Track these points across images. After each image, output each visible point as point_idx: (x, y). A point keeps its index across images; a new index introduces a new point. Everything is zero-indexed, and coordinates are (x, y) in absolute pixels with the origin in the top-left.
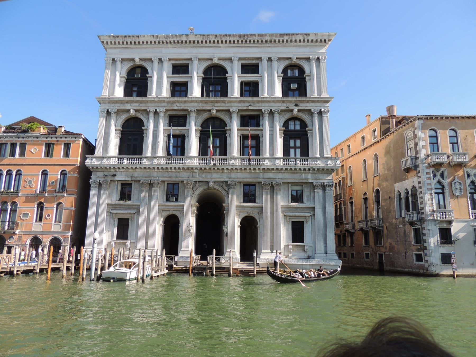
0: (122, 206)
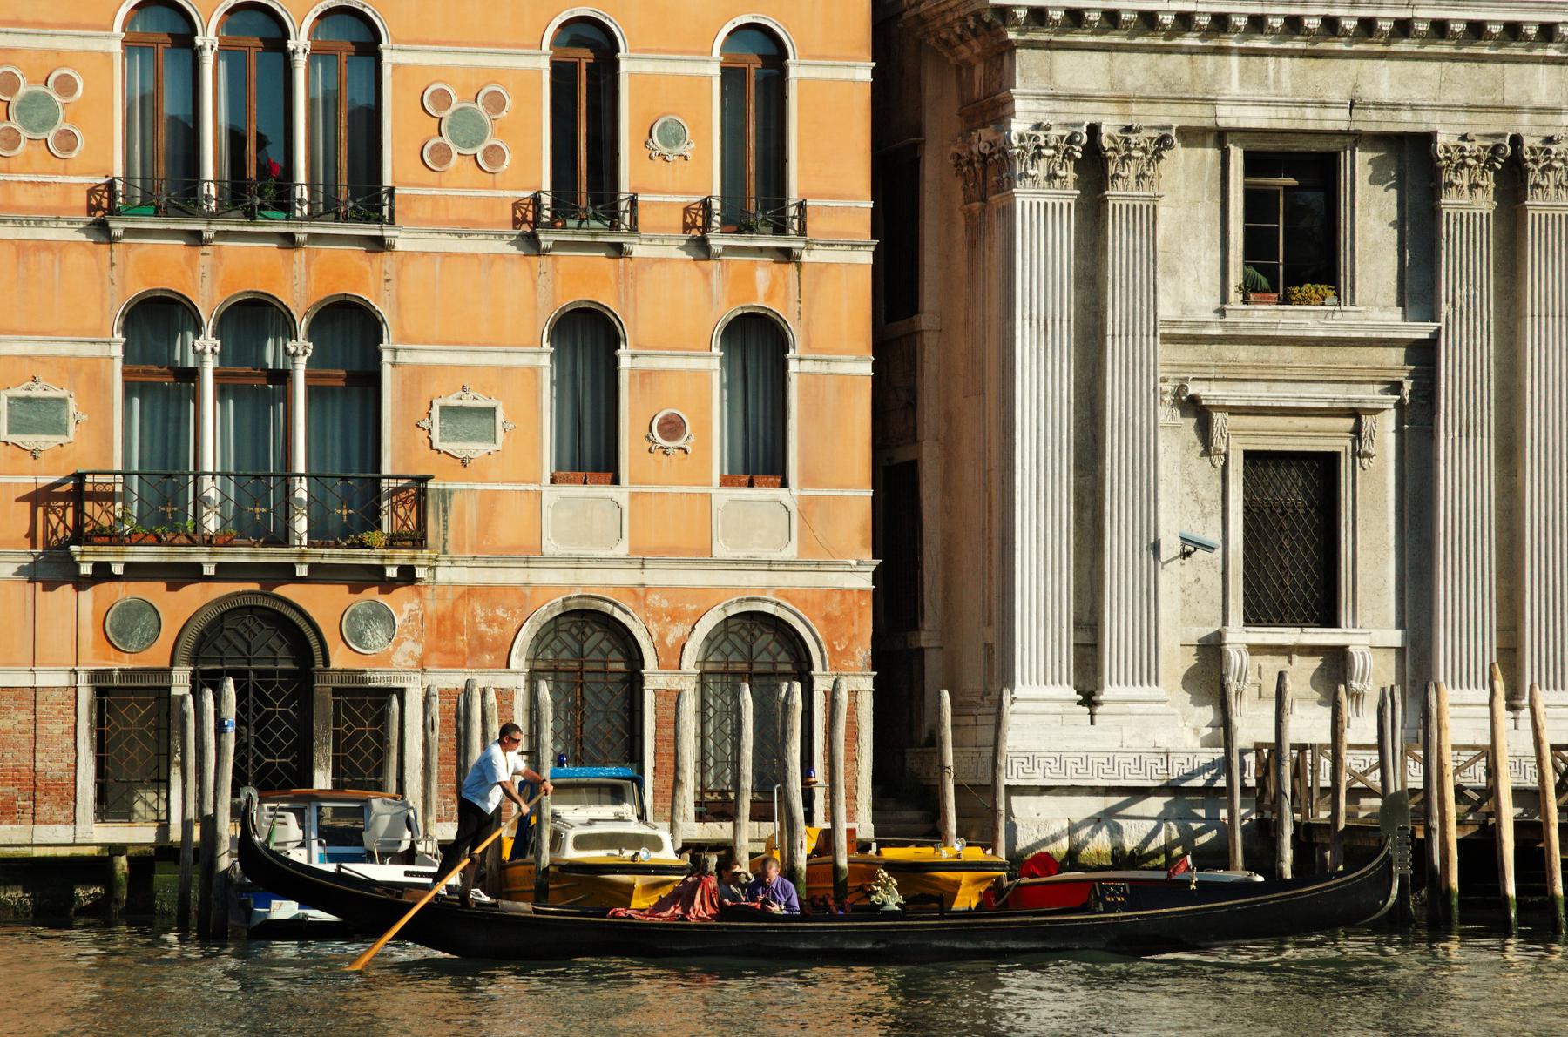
0: (1274, 354)
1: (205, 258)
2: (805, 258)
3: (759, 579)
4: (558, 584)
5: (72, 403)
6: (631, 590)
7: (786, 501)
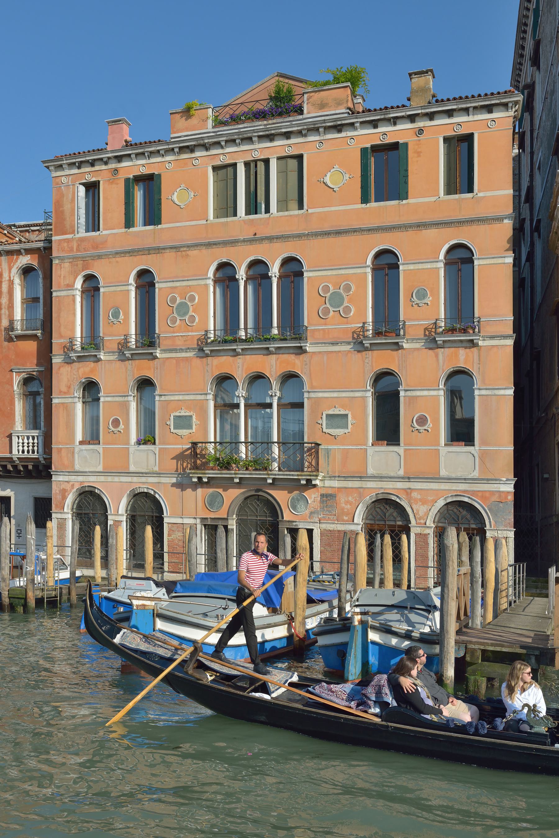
1: (240, 360)
2: (480, 343)
3: (463, 487)
4: (374, 488)
5: (194, 417)
6: (405, 490)
7: (473, 452)
